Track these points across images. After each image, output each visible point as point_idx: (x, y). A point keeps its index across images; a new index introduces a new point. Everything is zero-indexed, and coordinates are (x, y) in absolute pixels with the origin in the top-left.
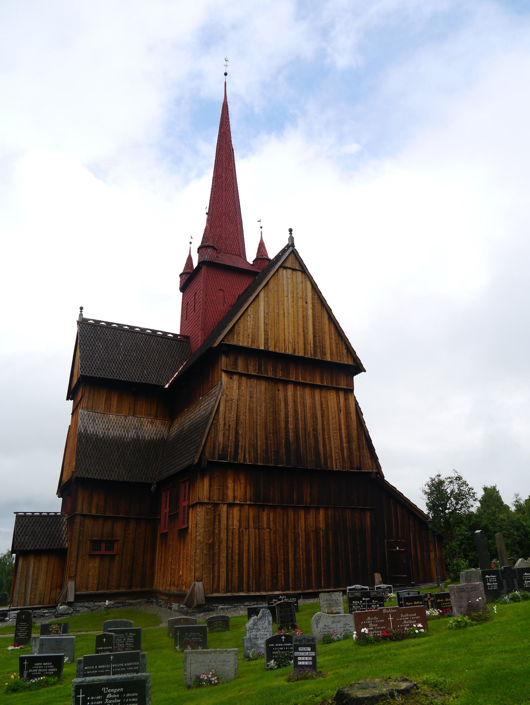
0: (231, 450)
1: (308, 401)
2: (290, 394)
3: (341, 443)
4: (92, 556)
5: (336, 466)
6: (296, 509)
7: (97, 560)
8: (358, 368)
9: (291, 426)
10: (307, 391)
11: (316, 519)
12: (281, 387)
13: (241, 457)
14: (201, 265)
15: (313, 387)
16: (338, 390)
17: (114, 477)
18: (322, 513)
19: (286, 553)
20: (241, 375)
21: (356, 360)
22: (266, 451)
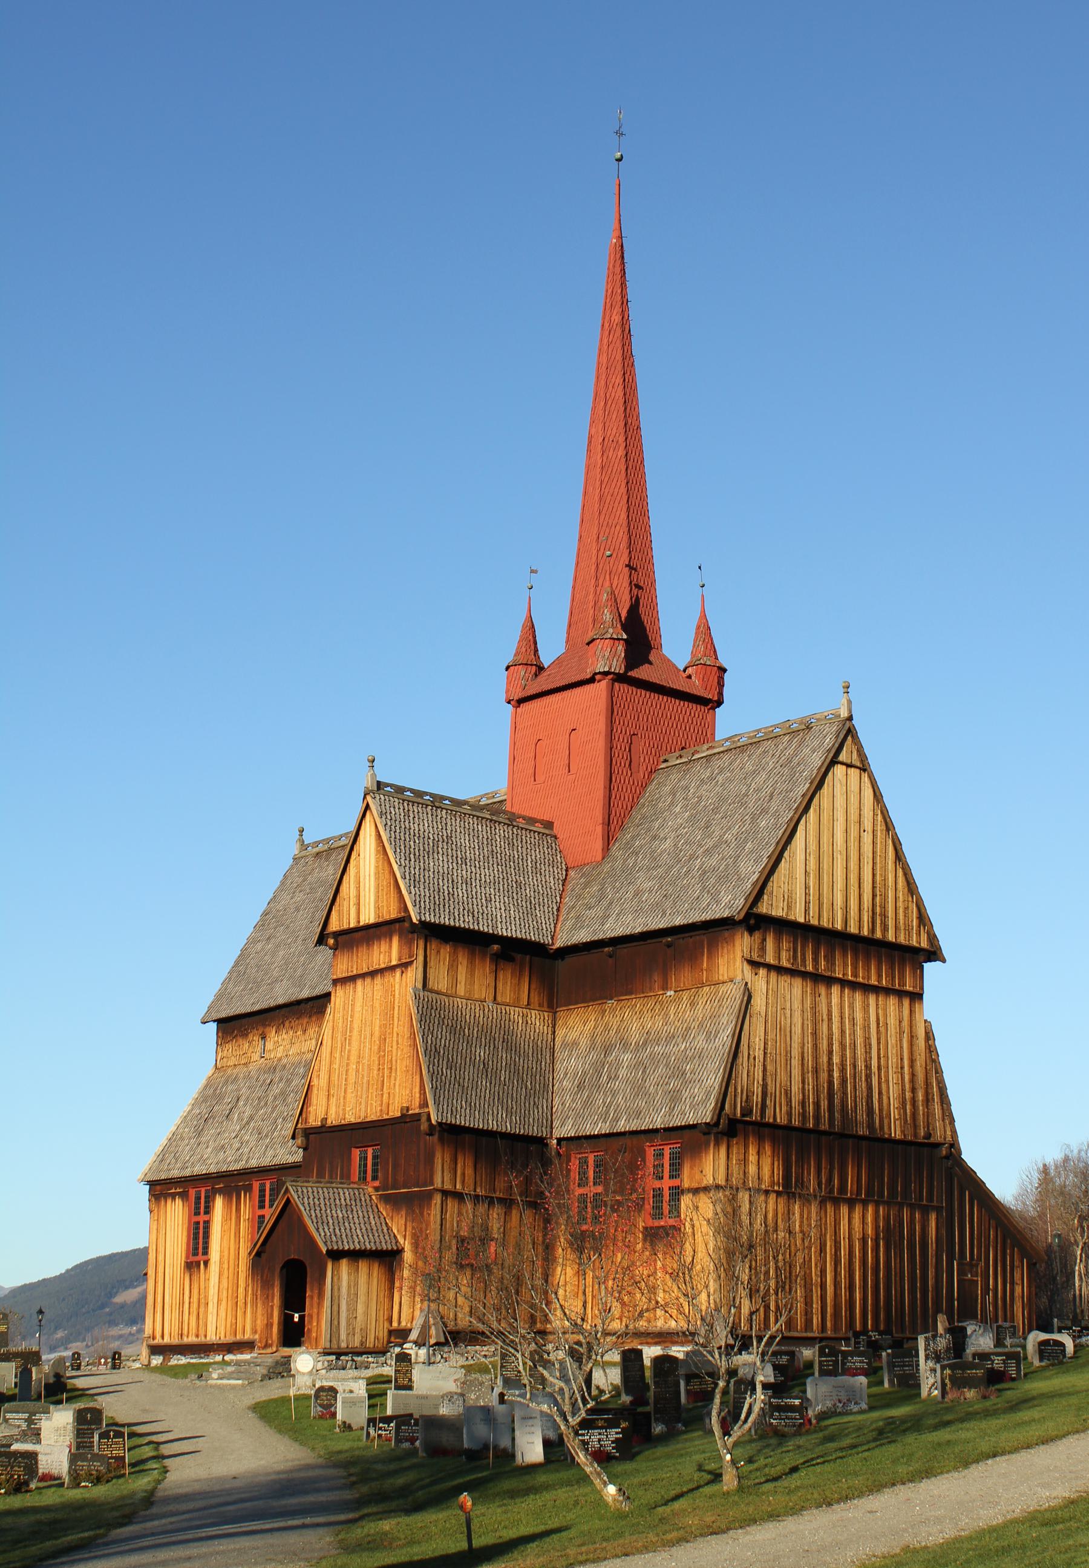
0: (757, 1098)
1: (859, 1015)
2: (835, 1000)
3: (903, 1090)
4: (461, 1267)
5: (896, 1133)
6: (836, 1202)
7: (468, 1272)
8: (934, 954)
9: (836, 1059)
10: (858, 996)
11: (864, 1217)
12: (823, 990)
13: (769, 1112)
14: (598, 677)
15: (867, 989)
16: (900, 994)
17: (492, 1125)
18: (870, 1209)
19: (823, 1272)
20: (769, 967)
21: (933, 938)
22: (803, 1103)
